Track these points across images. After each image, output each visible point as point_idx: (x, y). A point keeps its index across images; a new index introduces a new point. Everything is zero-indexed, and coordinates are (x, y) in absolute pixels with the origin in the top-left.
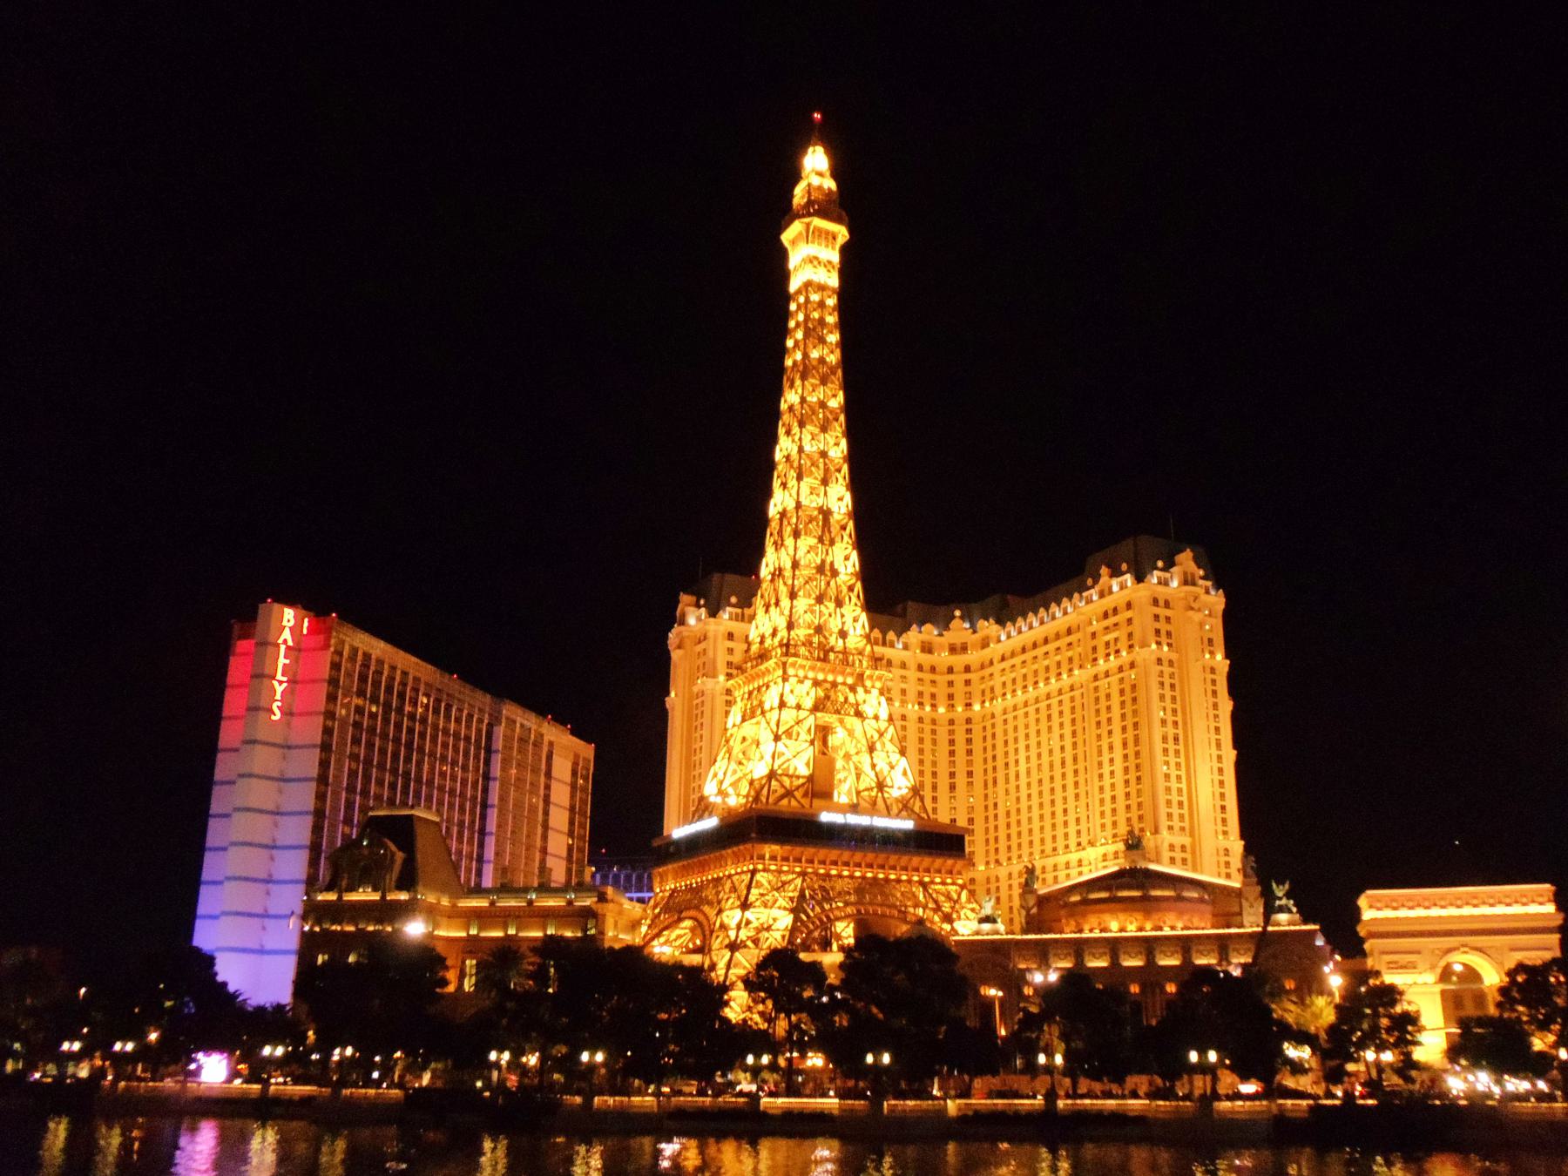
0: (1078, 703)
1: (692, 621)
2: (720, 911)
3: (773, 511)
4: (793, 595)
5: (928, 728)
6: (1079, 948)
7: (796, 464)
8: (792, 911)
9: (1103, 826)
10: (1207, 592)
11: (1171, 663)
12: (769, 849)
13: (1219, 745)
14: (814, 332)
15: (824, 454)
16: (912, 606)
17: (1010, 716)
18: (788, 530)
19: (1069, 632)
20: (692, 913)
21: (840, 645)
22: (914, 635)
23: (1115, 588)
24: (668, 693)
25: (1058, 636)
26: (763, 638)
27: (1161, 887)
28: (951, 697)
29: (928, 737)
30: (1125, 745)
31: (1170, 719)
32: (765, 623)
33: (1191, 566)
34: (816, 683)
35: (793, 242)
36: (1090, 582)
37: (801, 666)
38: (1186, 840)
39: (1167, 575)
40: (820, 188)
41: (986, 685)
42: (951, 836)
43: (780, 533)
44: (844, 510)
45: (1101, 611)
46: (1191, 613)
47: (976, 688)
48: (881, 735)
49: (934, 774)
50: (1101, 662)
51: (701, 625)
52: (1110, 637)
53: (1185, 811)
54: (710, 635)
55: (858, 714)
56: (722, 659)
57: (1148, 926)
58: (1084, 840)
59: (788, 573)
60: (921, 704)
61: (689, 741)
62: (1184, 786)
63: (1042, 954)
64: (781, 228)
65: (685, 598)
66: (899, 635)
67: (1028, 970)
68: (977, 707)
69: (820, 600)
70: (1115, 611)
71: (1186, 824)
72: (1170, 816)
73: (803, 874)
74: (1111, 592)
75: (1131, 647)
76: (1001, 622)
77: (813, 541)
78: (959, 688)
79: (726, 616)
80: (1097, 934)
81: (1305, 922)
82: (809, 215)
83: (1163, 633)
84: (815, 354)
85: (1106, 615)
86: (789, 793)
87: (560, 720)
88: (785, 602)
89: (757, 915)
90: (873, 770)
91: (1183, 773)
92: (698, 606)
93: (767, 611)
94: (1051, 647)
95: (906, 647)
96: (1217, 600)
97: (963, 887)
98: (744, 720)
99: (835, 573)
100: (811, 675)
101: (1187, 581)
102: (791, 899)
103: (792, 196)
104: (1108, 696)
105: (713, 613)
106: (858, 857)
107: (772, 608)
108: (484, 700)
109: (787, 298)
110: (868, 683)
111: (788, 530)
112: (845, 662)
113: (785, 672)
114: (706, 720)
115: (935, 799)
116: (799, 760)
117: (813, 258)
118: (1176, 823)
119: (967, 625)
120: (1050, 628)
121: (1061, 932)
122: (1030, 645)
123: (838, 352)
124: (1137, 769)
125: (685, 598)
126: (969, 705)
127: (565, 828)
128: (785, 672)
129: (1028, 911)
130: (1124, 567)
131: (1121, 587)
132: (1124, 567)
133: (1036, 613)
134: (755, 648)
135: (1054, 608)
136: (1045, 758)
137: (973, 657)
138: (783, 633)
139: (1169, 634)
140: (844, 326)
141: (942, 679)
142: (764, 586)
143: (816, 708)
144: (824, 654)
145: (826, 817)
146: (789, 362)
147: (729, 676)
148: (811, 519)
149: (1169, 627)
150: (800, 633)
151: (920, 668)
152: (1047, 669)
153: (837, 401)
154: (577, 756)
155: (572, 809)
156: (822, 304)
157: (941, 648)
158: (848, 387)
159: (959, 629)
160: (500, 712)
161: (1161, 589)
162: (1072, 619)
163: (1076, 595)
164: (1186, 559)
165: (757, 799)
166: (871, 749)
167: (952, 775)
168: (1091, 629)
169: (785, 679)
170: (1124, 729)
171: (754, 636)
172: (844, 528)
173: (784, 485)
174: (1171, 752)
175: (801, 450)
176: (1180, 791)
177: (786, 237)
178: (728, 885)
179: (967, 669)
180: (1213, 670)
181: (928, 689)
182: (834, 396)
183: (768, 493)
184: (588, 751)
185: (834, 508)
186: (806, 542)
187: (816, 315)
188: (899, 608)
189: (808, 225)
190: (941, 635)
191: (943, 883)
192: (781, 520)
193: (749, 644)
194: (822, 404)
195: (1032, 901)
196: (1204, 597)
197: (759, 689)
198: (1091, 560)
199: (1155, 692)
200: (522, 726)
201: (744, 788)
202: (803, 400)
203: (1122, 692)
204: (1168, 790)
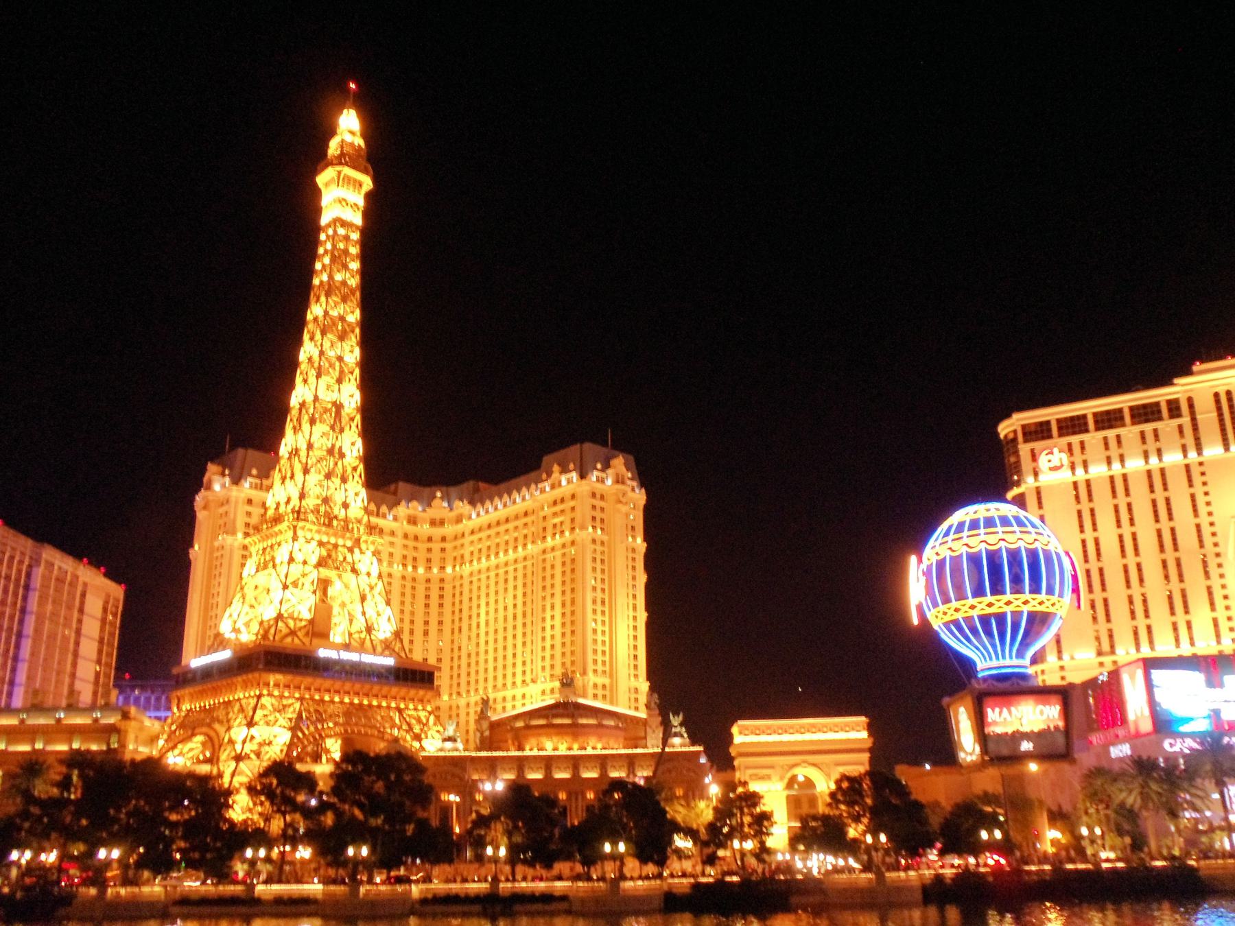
0: (529, 572)
1: (217, 487)
2: (229, 729)
3: (294, 401)
4: (306, 471)
5: (409, 585)
6: (521, 764)
7: (316, 365)
8: (291, 729)
9: (543, 668)
10: (633, 490)
11: (602, 543)
12: (273, 678)
13: (635, 608)
14: (339, 259)
15: (340, 359)
16: (402, 486)
17: (475, 579)
19: (526, 514)
20: (204, 729)
21: (342, 515)
22: (402, 510)
23: (564, 483)
24: (192, 546)
25: (517, 517)
26: (278, 504)
27: (586, 717)
28: (429, 560)
29: (408, 591)
30: (564, 605)
31: (599, 586)
32: (280, 493)
33: (623, 469)
34: (321, 544)
35: (327, 185)
36: (544, 476)
37: (309, 530)
38: (607, 681)
39: (604, 475)
40: (352, 144)
41: (457, 554)
42: (422, 672)
43: (299, 420)
44: (354, 405)
45: (551, 500)
46: (620, 506)
47: (450, 555)
48: (372, 588)
49: (412, 622)
50: (549, 539)
51: (224, 492)
52: (557, 520)
53: (607, 658)
54: (233, 500)
55: (354, 570)
56: (240, 521)
57: (576, 746)
58: (528, 678)
59: (303, 453)
60: (405, 565)
61: (208, 587)
62: (607, 639)
63: (491, 767)
64: (315, 172)
65: (212, 468)
66: (390, 509)
67: (482, 781)
68: (449, 570)
69: (328, 476)
70: (562, 500)
71: (607, 668)
72: (595, 662)
73: (301, 699)
74: (560, 485)
75: (573, 529)
76: (472, 503)
77: (326, 428)
78: (436, 555)
79: (247, 485)
80: (535, 752)
81: (693, 743)
82: (340, 164)
83: (598, 520)
84: (338, 277)
85: (555, 503)
86: (293, 633)
87: (96, 563)
88: (299, 475)
89: (260, 732)
90: (363, 617)
91: (607, 629)
92: (223, 475)
93: (283, 482)
94: (510, 526)
95: (395, 519)
96: (639, 497)
97: (430, 713)
98: (257, 571)
99: (342, 455)
100: (317, 537)
101: (619, 480)
102: (290, 720)
103: (327, 146)
104: (553, 567)
105: (236, 481)
106: (348, 686)
107: (288, 480)
108: (25, 544)
109: (318, 229)
110: (363, 546)
111: (305, 418)
112: (346, 528)
113: (295, 533)
114: (224, 570)
115: (411, 642)
116: (302, 606)
117: (342, 198)
118: (600, 667)
119: (445, 504)
120: (511, 510)
121: (508, 750)
122: (494, 523)
123: (358, 277)
124: (573, 624)
125: (212, 468)
126: (442, 568)
127: (94, 656)
128: (295, 533)
129: (482, 734)
130: (571, 466)
131: (568, 482)
132: (571, 466)
133: (501, 498)
134: (270, 513)
135: (515, 495)
136: (501, 613)
137: (449, 530)
138: (295, 502)
139: (602, 520)
140: (364, 257)
141: (423, 546)
142: (282, 462)
143: (321, 563)
144: (330, 519)
145: (323, 653)
146: (316, 281)
147: (247, 535)
148: (326, 410)
149: (603, 516)
150: (310, 502)
151: (406, 536)
152: (507, 543)
153: (354, 316)
154: (108, 596)
155: (101, 641)
156: (347, 238)
157: (424, 521)
158: (365, 306)
159: (440, 507)
160: (40, 556)
161: (599, 485)
162: (529, 504)
163: (533, 486)
164: (619, 463)
165: (265, 636)
166: (363, 599)
167: (426, 623)
168: (542, 514)
170: (564, 592)
171: (271, 504)
172: (352, 419)
173: (305, 381)
174: (599, 612)
175: (322, 353)
176: (604, 642)
177: (321, 180)
178: (237, 708)
179: (444, 539)
180: (634, 550)
181: (411, 554)
182: (353, 312)
183: (291, 385)
184: (117, 592)
185: (346, 404)
186: (320, 428)
187: (341, 246)
188: (392, 487)
189: (339, 173)
190: (424, 511)
191: (416, 709)
192: (300, 410)
193: (266, 509)
194: (342, 319)
195: (485, 725)
196: (630, 494)
197: (272, 546)
198: (545, 459)
199: (589, 565)
200: (60, 568)
201: (255, 627)
202: (326, 313)
203: (564, 564)
204: (595, 641)
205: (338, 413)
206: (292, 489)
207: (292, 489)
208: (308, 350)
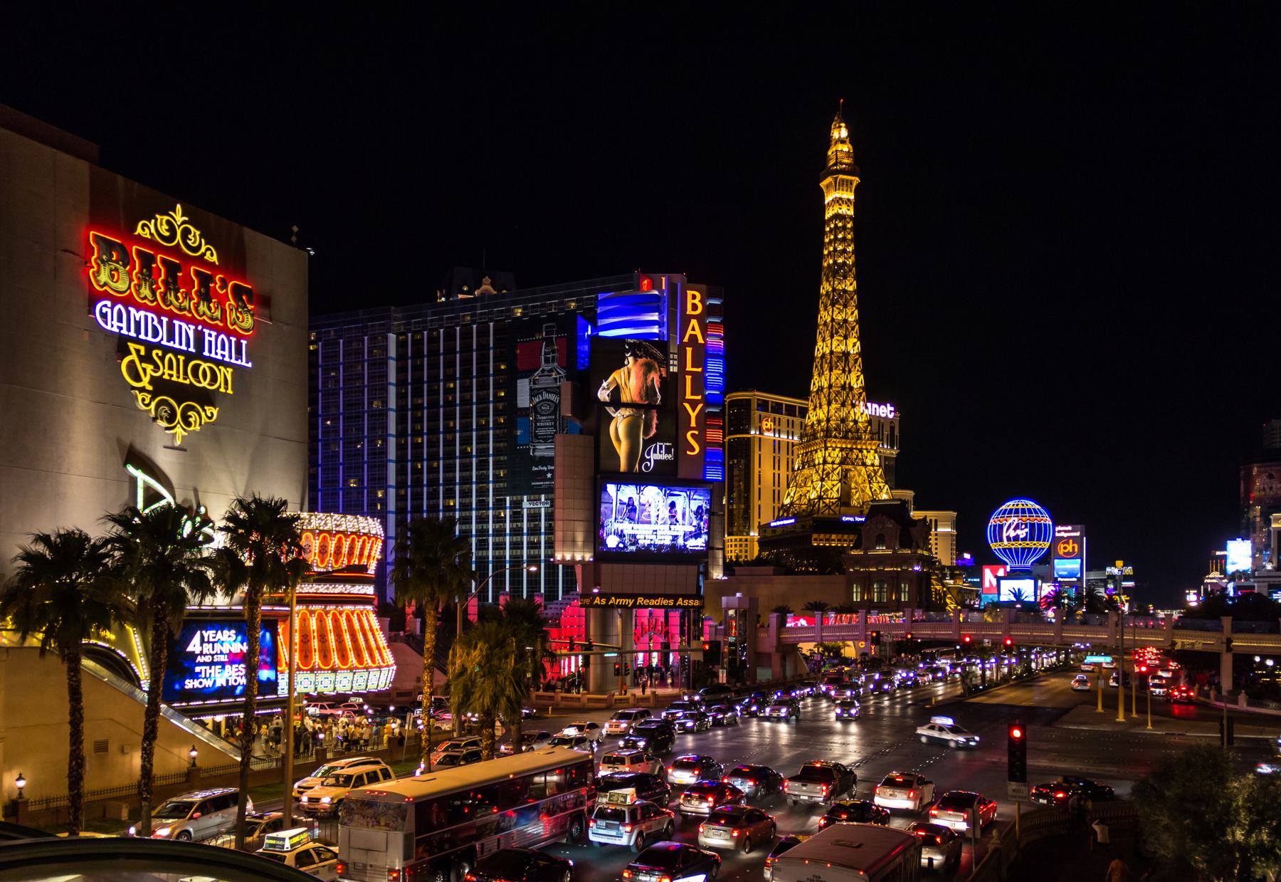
3: (818, 354)
4: (829, 404)
15: (845, 321)
34: (842, 449)
69: (843, 405)
88: (825, 407)
99: (851, 388)
143: (841, 463)
169: (826, 448)
172: (856, 361)
186: (835, 372)
205: (847, 359)
208: (824, 316)
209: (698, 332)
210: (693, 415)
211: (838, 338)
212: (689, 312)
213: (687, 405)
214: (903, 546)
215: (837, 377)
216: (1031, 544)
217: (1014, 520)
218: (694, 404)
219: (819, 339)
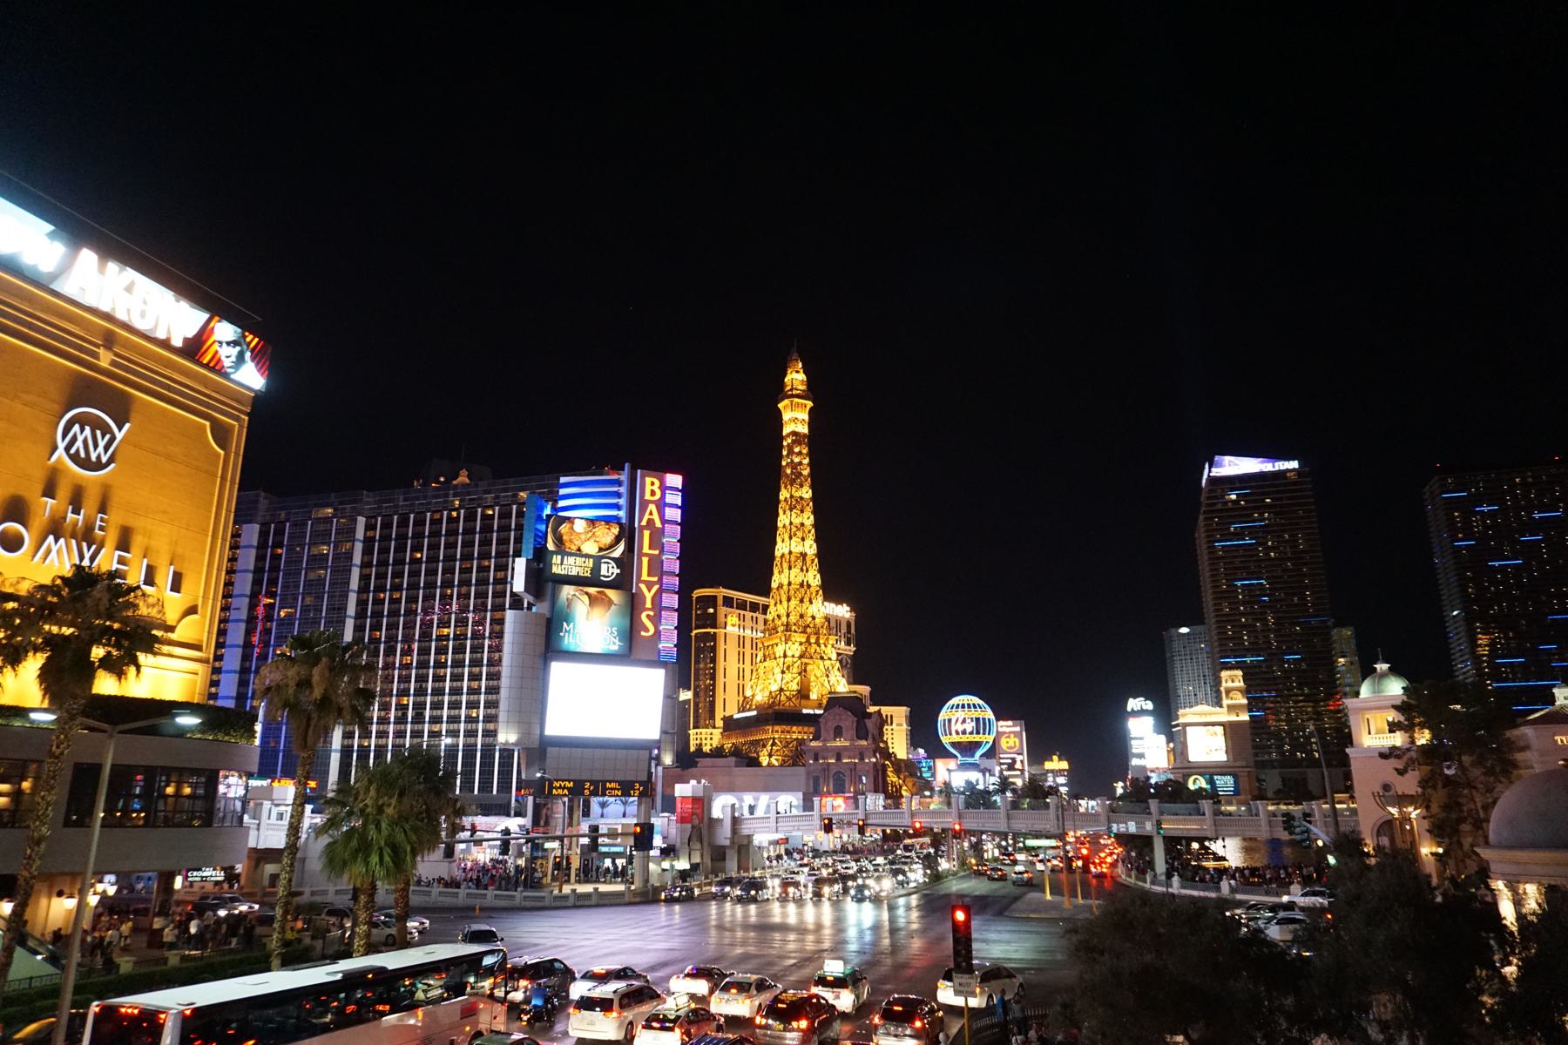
3: (778, 554)
4: (789, 600)
18: (785, 565)
69: (802, 601)
86: (789, 699)
99: (809, 586)
109: (782, 438)
117: (795, 418)
138: (784, 619)
143: (801, 657)
150: (793, 619)
177: (780, 406)
186: (795, 571)
206: (782, 610)
207: (782, 610)
208: (783, 520)
209: (656, 517)
210: (649, 596)
211: (796, 537)
212: (648, 496)
213: (643, 587)
214: (859, 738)
215: (796, 576)
216: (977, 738)
217: (961, 714)
218: (649, 586)
219: (779, 539)
